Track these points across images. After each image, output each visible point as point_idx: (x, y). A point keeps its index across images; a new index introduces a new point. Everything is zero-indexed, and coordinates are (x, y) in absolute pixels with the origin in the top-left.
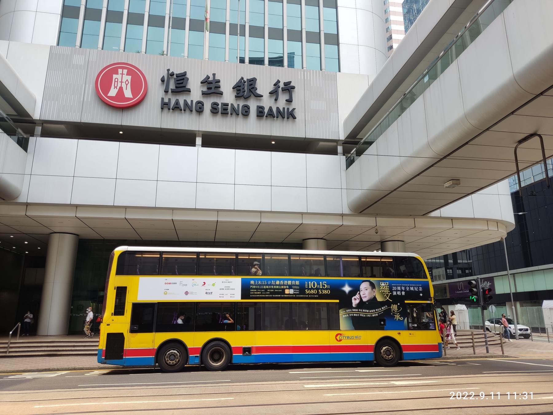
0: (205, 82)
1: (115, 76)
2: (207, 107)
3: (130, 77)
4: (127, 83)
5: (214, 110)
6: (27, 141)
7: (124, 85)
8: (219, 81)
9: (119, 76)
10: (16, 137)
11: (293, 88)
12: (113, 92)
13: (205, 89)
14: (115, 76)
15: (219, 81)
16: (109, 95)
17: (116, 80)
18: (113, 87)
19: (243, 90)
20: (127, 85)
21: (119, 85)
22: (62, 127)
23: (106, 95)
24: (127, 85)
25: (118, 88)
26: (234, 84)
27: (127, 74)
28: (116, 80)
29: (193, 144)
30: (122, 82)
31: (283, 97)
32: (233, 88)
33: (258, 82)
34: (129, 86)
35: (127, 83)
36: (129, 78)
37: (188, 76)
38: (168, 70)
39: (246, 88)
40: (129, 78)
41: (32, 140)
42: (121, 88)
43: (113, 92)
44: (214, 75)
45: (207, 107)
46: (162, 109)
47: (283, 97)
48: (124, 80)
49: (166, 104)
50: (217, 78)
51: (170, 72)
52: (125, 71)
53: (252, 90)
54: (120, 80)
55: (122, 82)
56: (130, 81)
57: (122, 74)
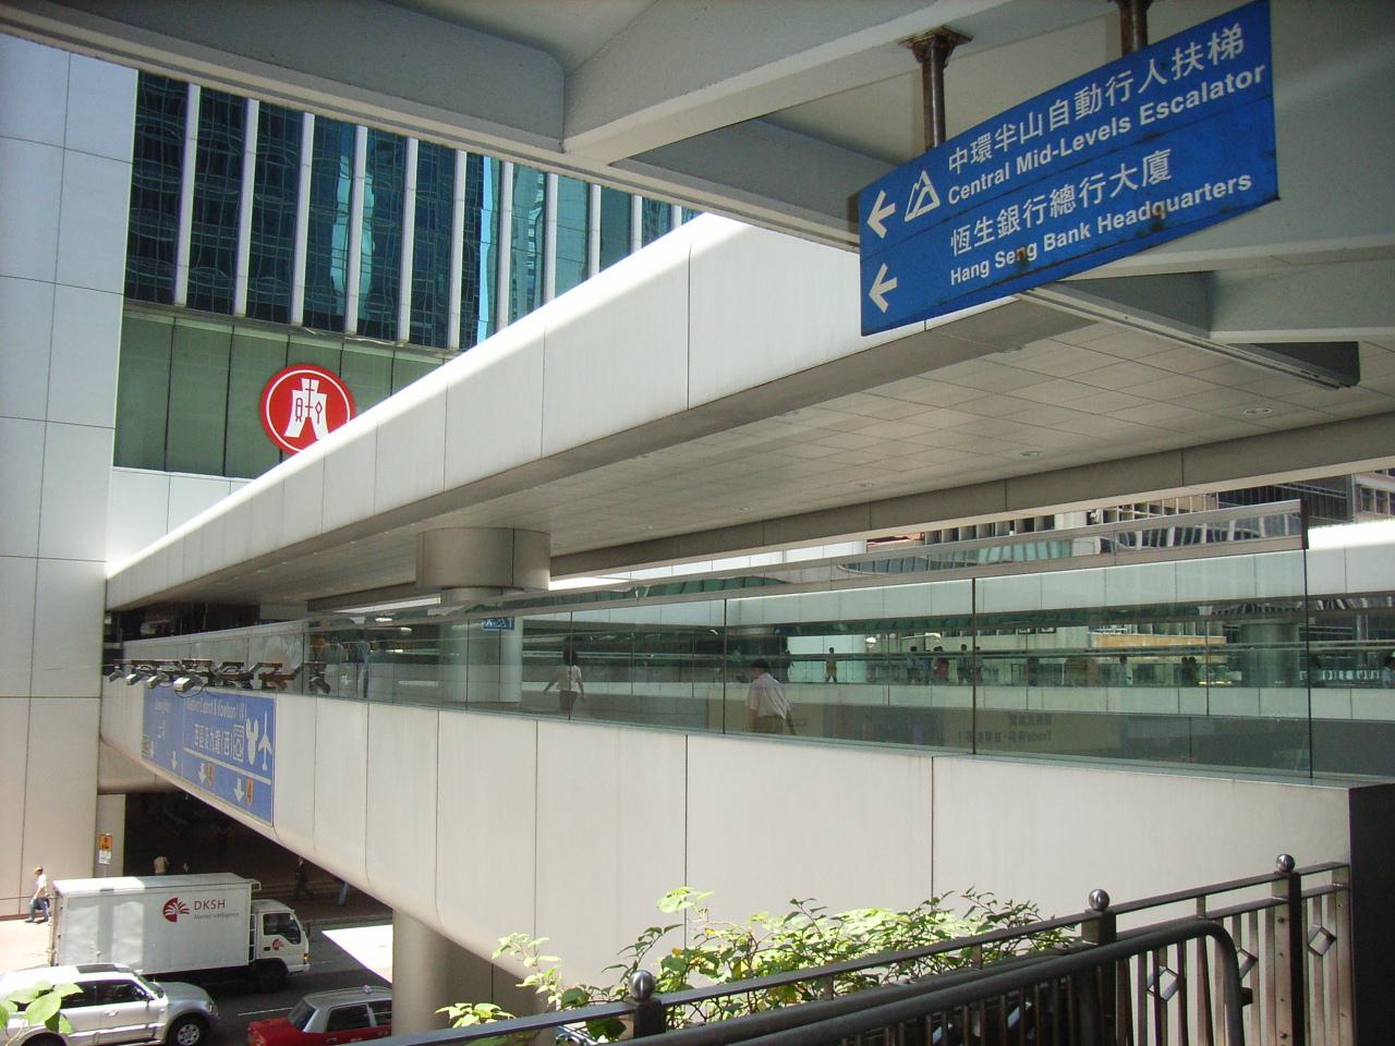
3: (325, 396)
4: (319, 408)
14: (296, 394)
16: (286, 435)
17: (299, 403)
19: (433, 341)
21: (305, 415)
23: (282, 433)
25: (303, 419)
27: (320, 391)
28: (299, 403)
34: (324, 411)
35: (319, 408)
36: (323, 398)
40: (323, 398)
42: (308, 420)
48: (313, 404)
52: (315, 384)
54: (306, 403)
55: (309, 407)
56: (324, 405)
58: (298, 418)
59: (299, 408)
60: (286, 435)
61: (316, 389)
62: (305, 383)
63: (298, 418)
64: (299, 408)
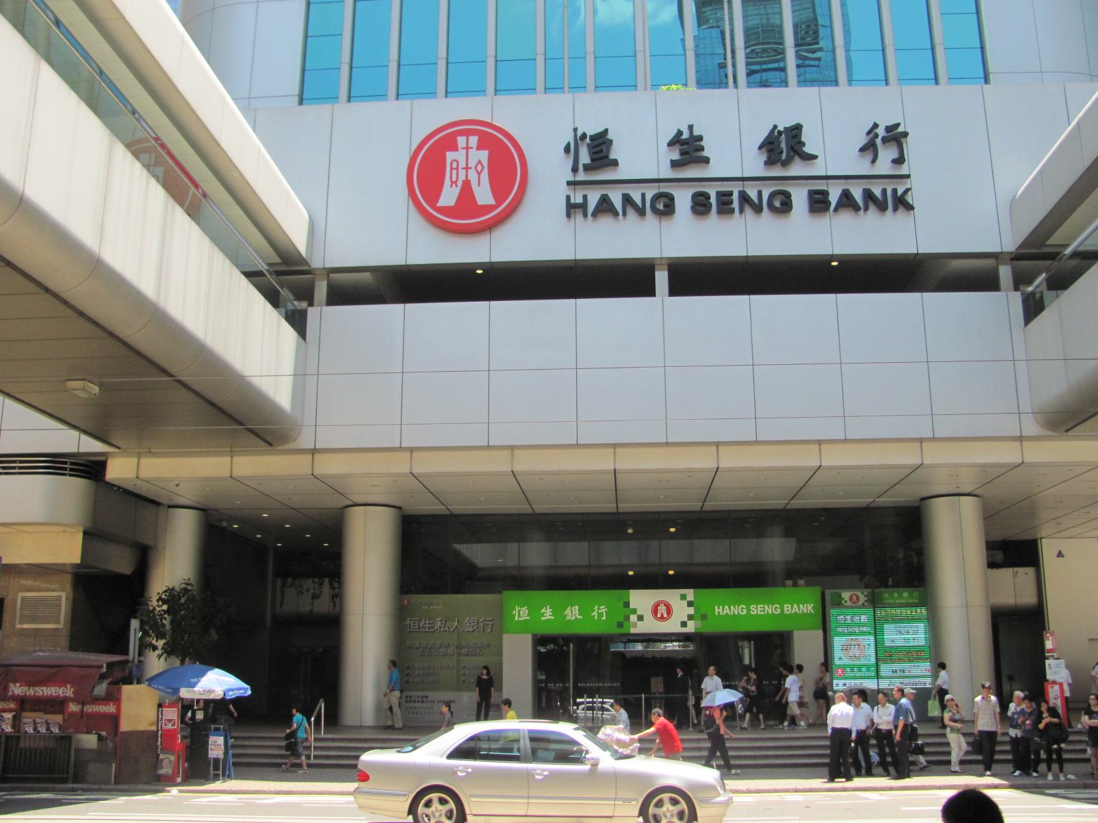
0: (676, 141)
1: (450, 156)
2: (683, 199)
4: (479, 168)
5: (700, 205)
6: (303, 314)
7: (473, 176)
8: (700, 138)
9: (459, 155)
10: (283, 310)
11: (905, 134)
12: (449, 196)
13: (676, 156)
14: (450, 156)
15: (700, 138)
16: (440, 204)
17: (455, 165)
18: (447, 182)
20: (479, 174)
21: (462, 177)
22: (367, 276)
24: (479, 174)
25: (460, 183)
26: (761, 138)
27: (479, 147)
28: (455, 165)
29: (650, 292)
30: (467, 168)
31: (887, 155)
32: (760, 148)
33: (804, 130)
34: (485, 174)
35: (479, 168)
36: (484, 155)
37: (610, 136)
38: (575, 130)
39: (783, 145)
40: (484, 155)
41: (313, 313)
42: (467, 183)
43: (449, 196)
44: (691, 127)
45: (683, 199)
46: (568, 215)
47: (887, 155)
48: (472, 164)
49: (576, 206)
50: (696, 133)
51: (579, 133)
52: (474, 140)
53: (796, 147)
54: (462, 164)
56: (485, 163)
57: (467, 148)
58: (453, 183)
59: (454, 172)
60: (440, 204)
61: (475, 147)
62: (461, 141)
63: (453, 183)
64: (454, 172)
